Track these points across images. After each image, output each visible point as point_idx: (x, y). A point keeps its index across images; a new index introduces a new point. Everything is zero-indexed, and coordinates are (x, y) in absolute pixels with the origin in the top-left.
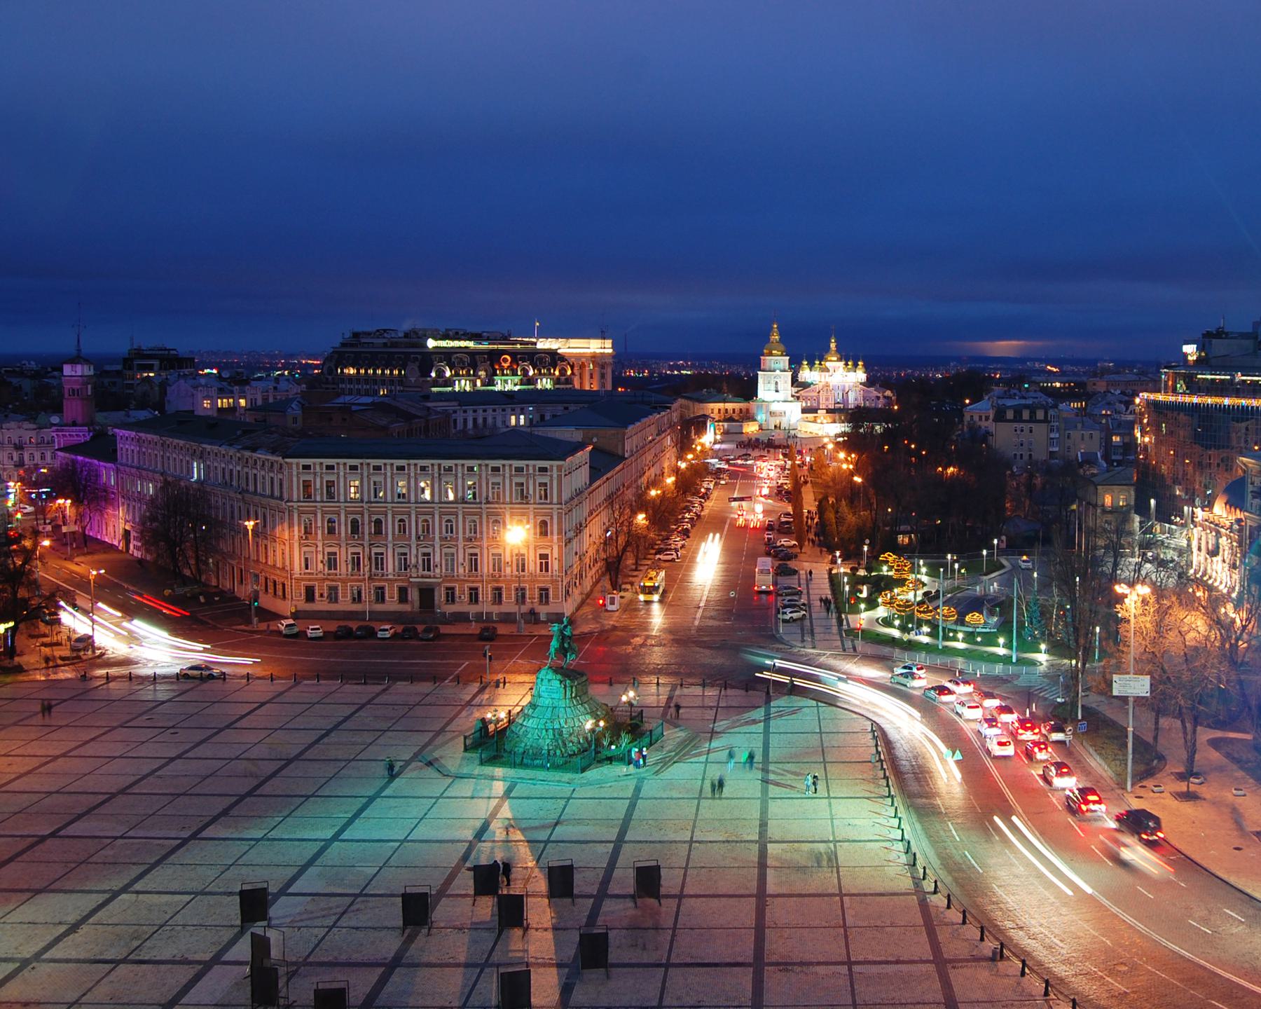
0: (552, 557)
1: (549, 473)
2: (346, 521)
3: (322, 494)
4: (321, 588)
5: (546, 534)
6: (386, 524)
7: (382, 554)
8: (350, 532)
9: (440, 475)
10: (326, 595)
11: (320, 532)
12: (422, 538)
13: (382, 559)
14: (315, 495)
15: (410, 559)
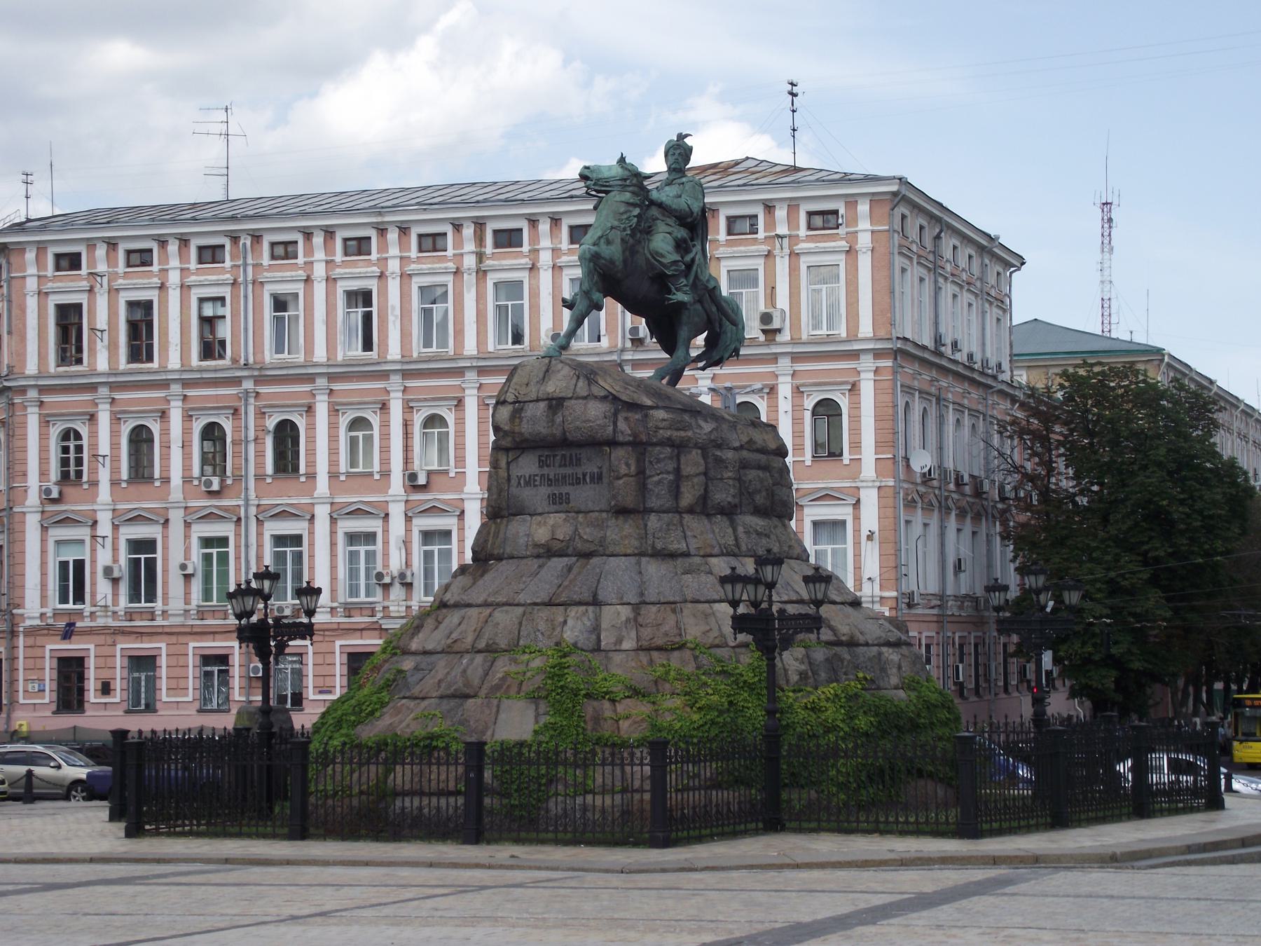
0: (857, 531)
1: (841, 231)
2: (186, 432)
3: (112, 347)
4: (106, 660)
5: (836, 454)
6: (311, 439)
7: (296, 540)
8: (196, 471)
9: (480, 257)
10: (118, 685)
11: (104, 476)
12: (422, 480)
13: (298, 557)
14: (92, 351)
15: (386, 555)
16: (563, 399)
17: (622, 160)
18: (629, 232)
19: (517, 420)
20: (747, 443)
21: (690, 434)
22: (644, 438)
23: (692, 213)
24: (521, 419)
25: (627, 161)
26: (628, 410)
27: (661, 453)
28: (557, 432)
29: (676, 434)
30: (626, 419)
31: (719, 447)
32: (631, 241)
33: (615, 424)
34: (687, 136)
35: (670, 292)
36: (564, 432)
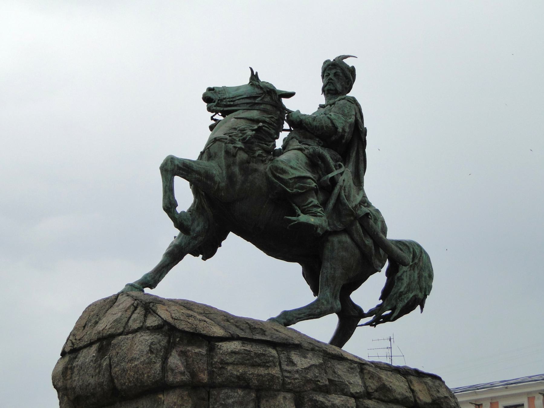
16: (112, 336)
17: (254, 77)
18: (240, 145)
19: (69, 372)
20: (376, 391)
21: (275, 371)
22: (204, 377)
23: (336, 128)
24: (72, 369)
25: (262, 78)
26: (190, 343)
27: (228, 397)
28: (104, 379)
29: (251, 371)
30: (183, 354)
31: (326, 390)
32: (242, 156)
33: (165, 360)
34: (346, 57)
35: (295, 214)
36: (111, 379)
